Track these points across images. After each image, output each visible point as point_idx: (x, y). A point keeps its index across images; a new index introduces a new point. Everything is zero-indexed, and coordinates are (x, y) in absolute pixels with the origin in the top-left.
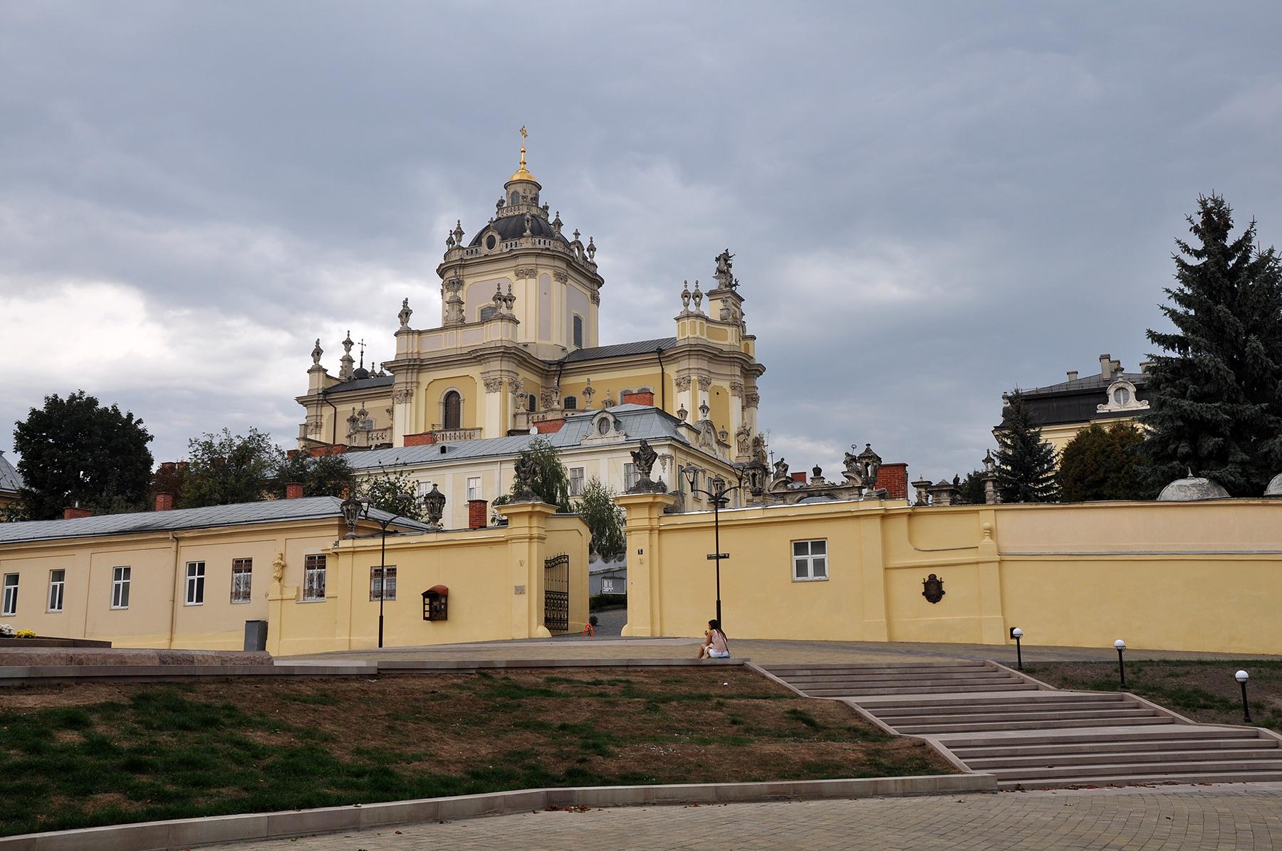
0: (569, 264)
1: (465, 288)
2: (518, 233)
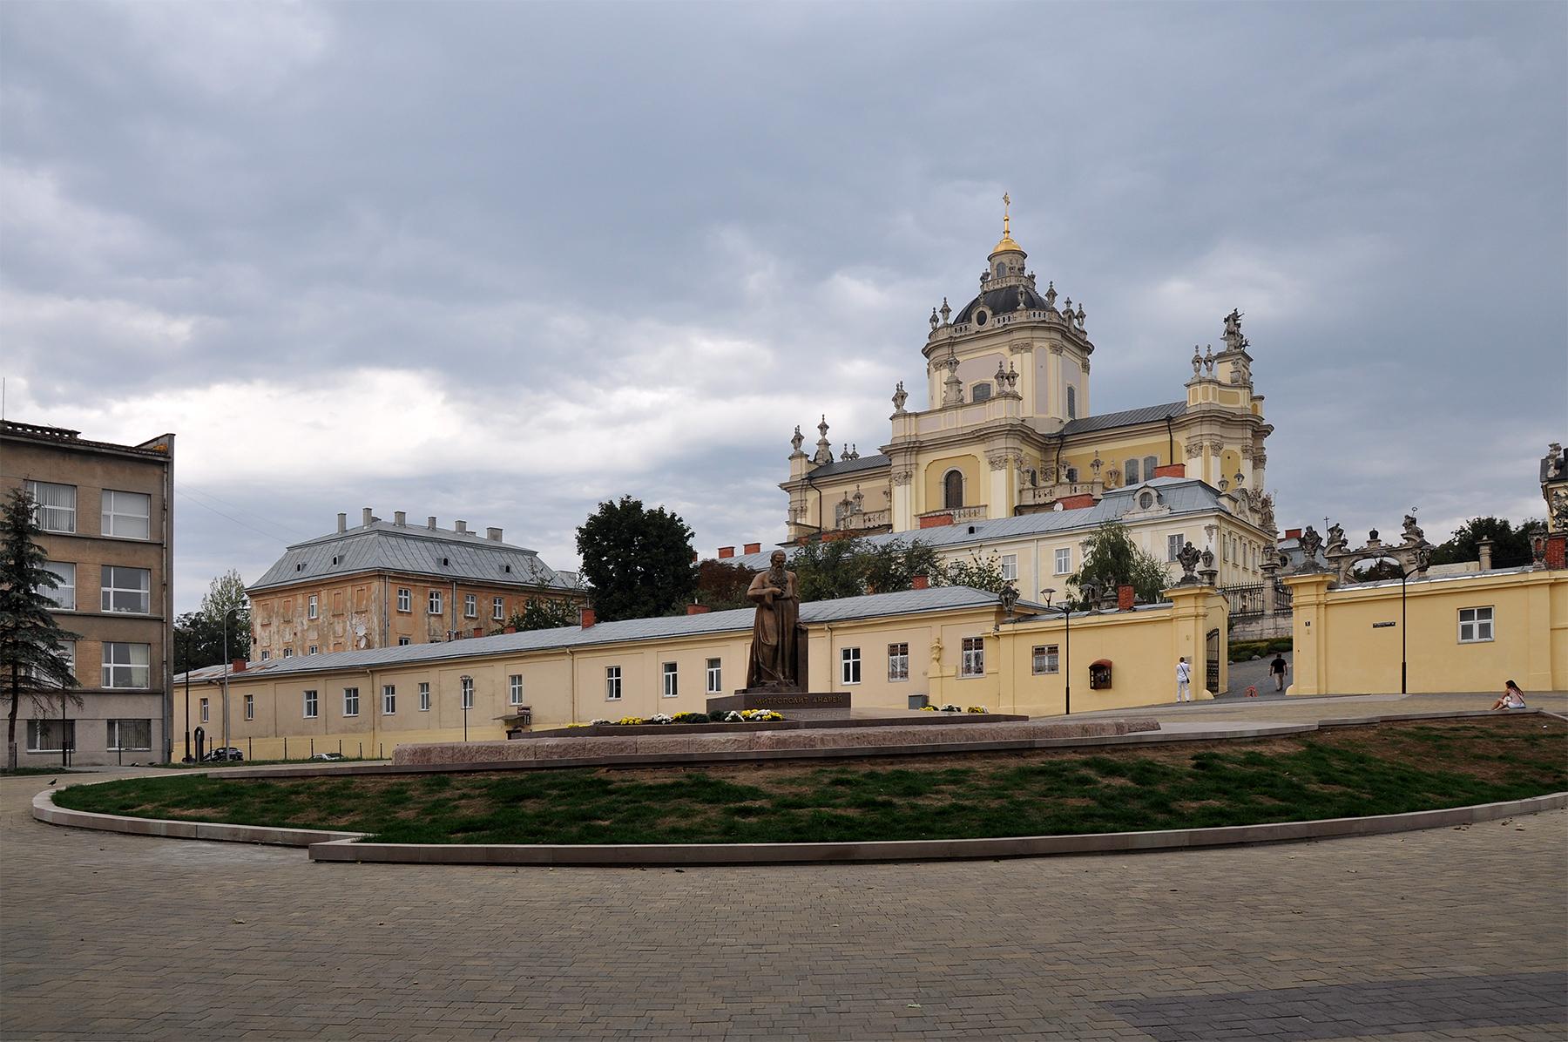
0: (1064, 335)
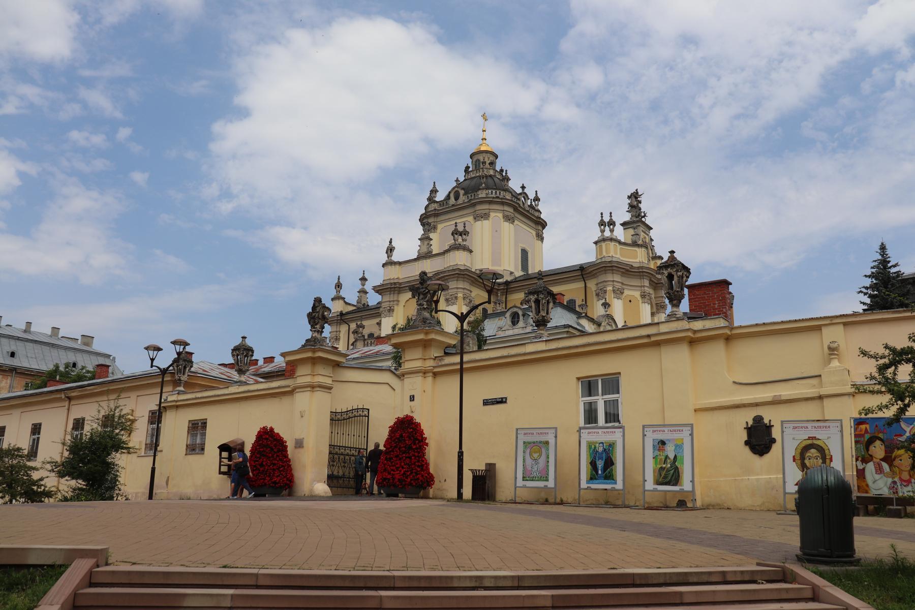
0: (516, 209)
1: (439, 230)
2: (476, 189)
